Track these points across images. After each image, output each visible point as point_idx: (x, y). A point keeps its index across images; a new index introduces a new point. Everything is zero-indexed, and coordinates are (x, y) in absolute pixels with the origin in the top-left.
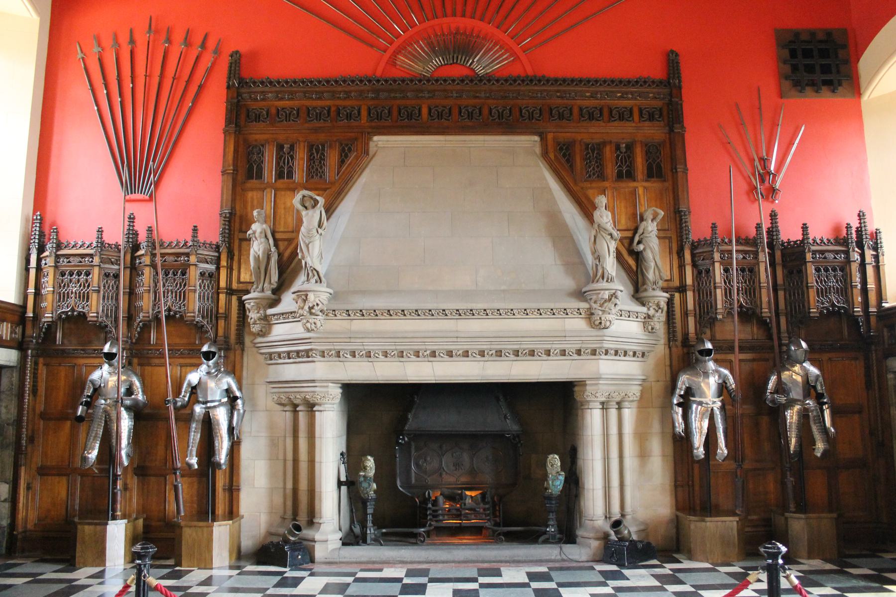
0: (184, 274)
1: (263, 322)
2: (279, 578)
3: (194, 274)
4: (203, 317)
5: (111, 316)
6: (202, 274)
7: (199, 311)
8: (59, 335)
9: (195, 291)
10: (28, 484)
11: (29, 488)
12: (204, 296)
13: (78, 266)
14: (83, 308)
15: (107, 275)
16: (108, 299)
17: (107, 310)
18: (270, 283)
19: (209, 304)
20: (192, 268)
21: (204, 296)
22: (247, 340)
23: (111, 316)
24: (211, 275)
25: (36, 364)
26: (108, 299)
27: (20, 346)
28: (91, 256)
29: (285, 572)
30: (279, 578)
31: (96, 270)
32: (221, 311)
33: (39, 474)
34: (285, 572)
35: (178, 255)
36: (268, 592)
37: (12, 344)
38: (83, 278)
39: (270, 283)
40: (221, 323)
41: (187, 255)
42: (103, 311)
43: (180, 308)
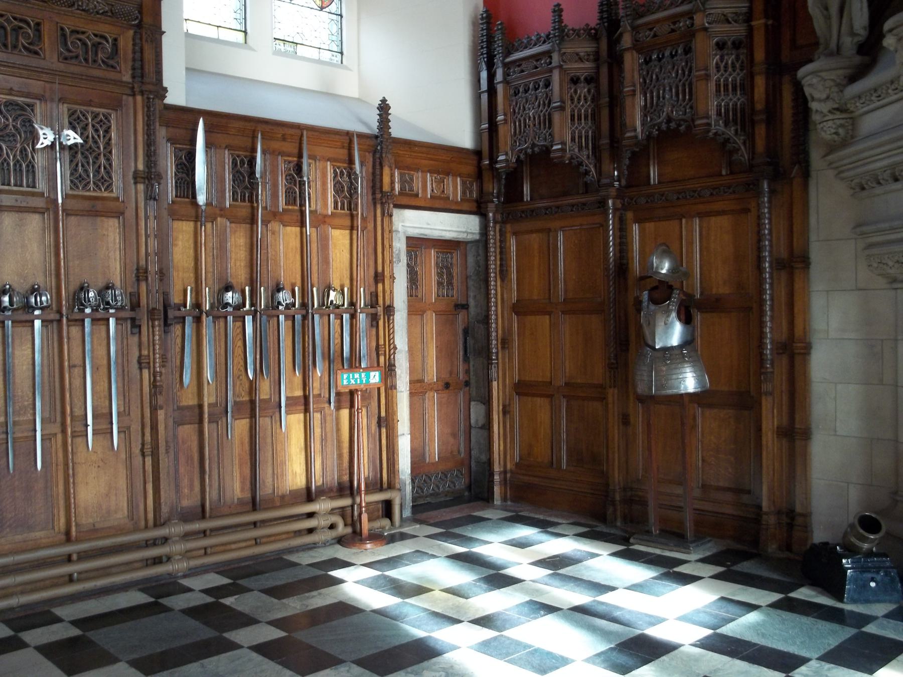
0: (688, 51)
1: (838, 115)
2: (848, 632)
3: (704, 47)
4: (726, 124)
5: (587, 147)
6: (720, 46)
7: (719, 114)
8: (527, 190)
9: (707, 77)
10: (504, 407)
11: (505, 411)
12: (726, 86)
13: (533, 75)
14: (545, 139)
15: (575, 81)
16: (580, 119)
17: (580, 137)
18: (853, 34)
19: (738, 99)
20: (700, 37)
21: (726, 86)
22: (815, 156)
23: (587, 147)
24: (737, 45)
25: (502, 233)
26: (580, 119)
27: (479, 209)
28: (548, 54)
29: (869, 619)
30: (848, 632)
31: (556, 77)
32: (759, 106)
33: (517, 393)
34: (869, 619)
35: (675, 19)
36: (871, 629)
37: (466, 207)
38: (541, 91)
39: (853, 34)
40: (761, 131)
41: (690, 15)
42: (573, 139)
43: (685, 113)
